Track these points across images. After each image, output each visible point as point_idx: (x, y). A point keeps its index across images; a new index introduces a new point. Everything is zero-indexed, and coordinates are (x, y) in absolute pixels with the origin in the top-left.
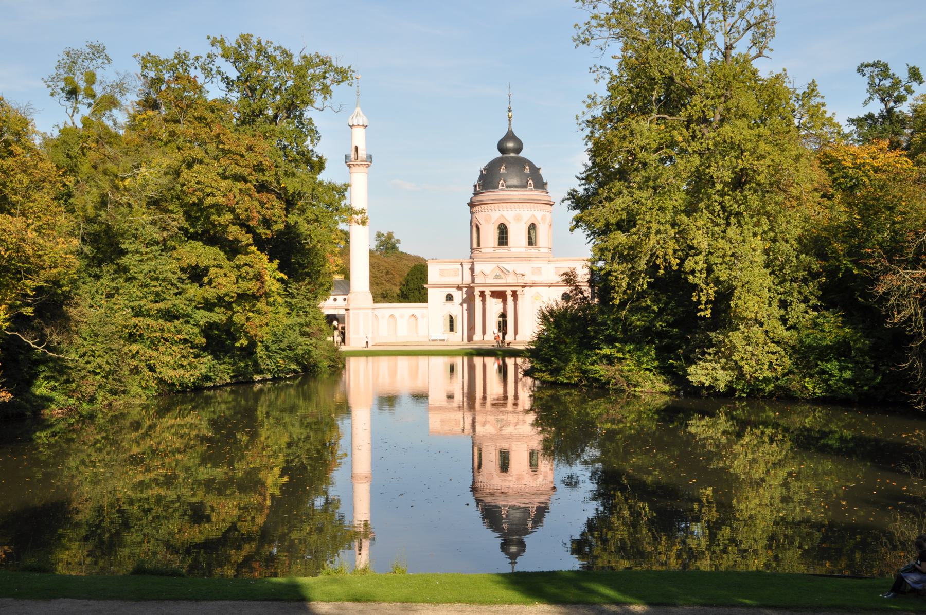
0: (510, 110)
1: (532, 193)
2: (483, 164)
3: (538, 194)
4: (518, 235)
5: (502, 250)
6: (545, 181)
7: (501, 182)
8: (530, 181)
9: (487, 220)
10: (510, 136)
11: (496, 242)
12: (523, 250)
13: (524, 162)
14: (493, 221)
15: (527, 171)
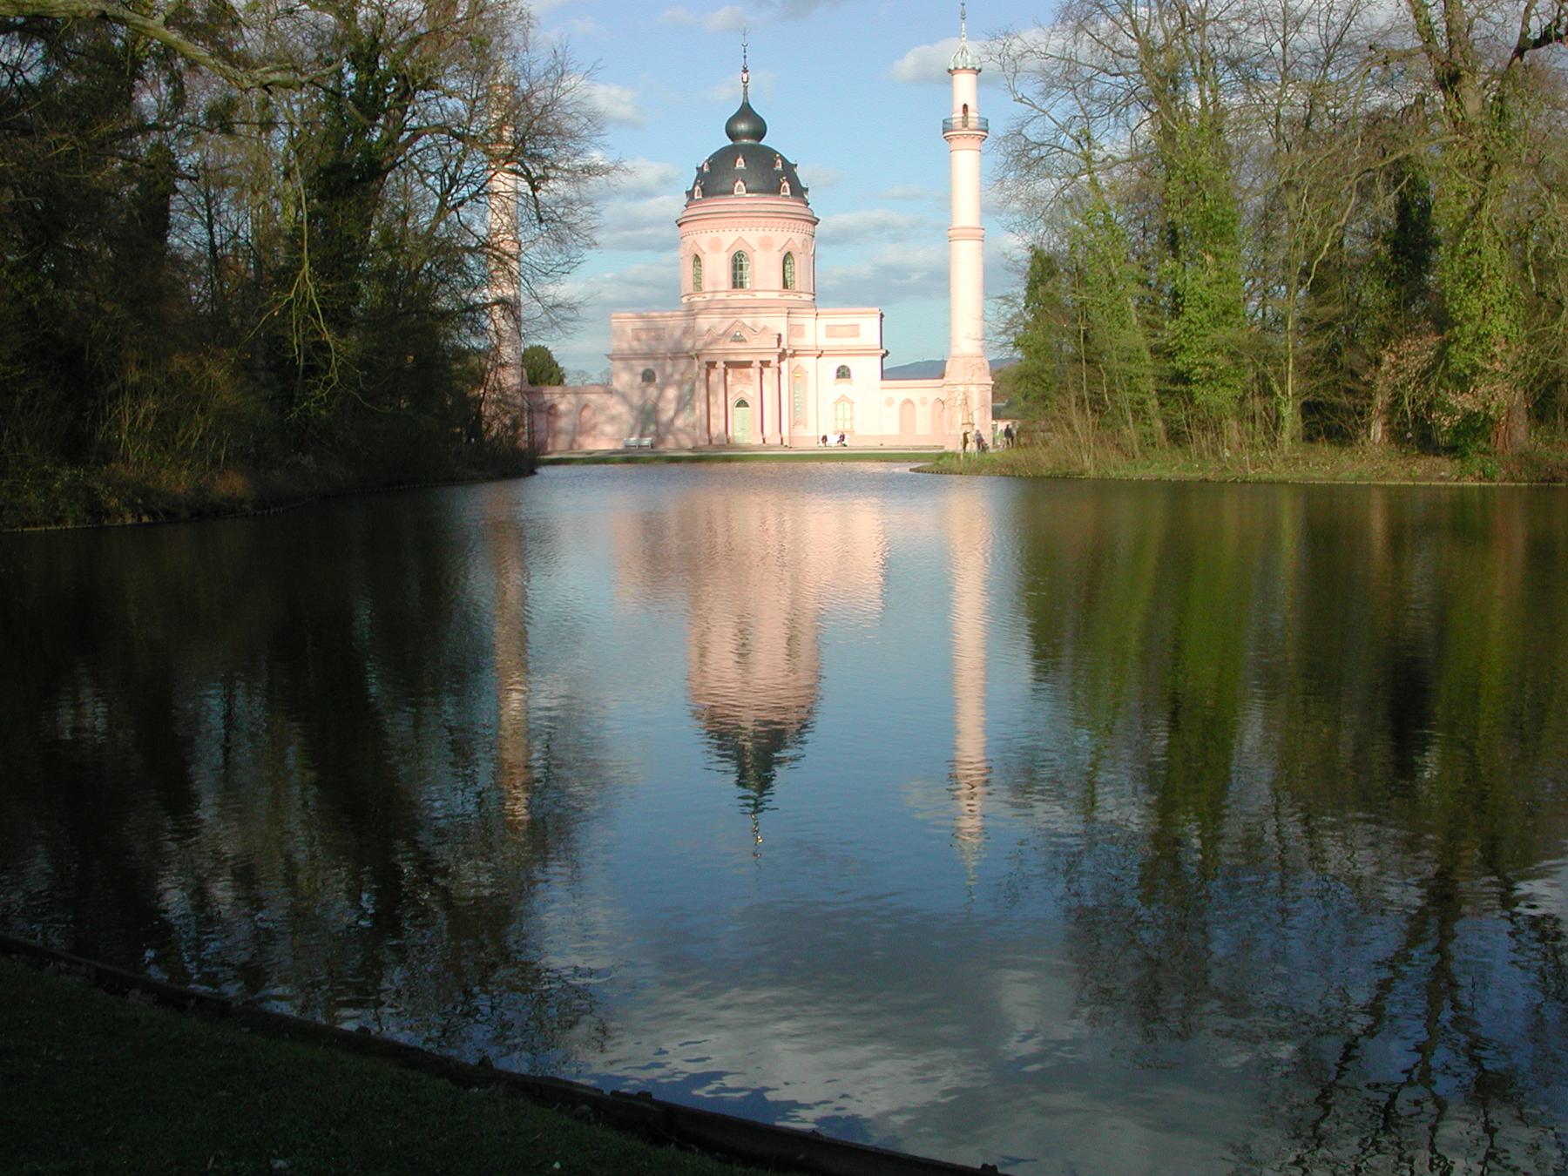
0: (745, 71)
1: (783, 202)
2: (702, 158)
3: (795, 206)
4: (764, 272)
5: (739, 296)
6: (804, 186)
7: (737, 185)
8: (786, 184)
9: (716, 246)
10: (746, 112)
11: (731, 285)
12: (775, 295)
13: (770, 154)
14: (726, 249)
15: (779, 167)
